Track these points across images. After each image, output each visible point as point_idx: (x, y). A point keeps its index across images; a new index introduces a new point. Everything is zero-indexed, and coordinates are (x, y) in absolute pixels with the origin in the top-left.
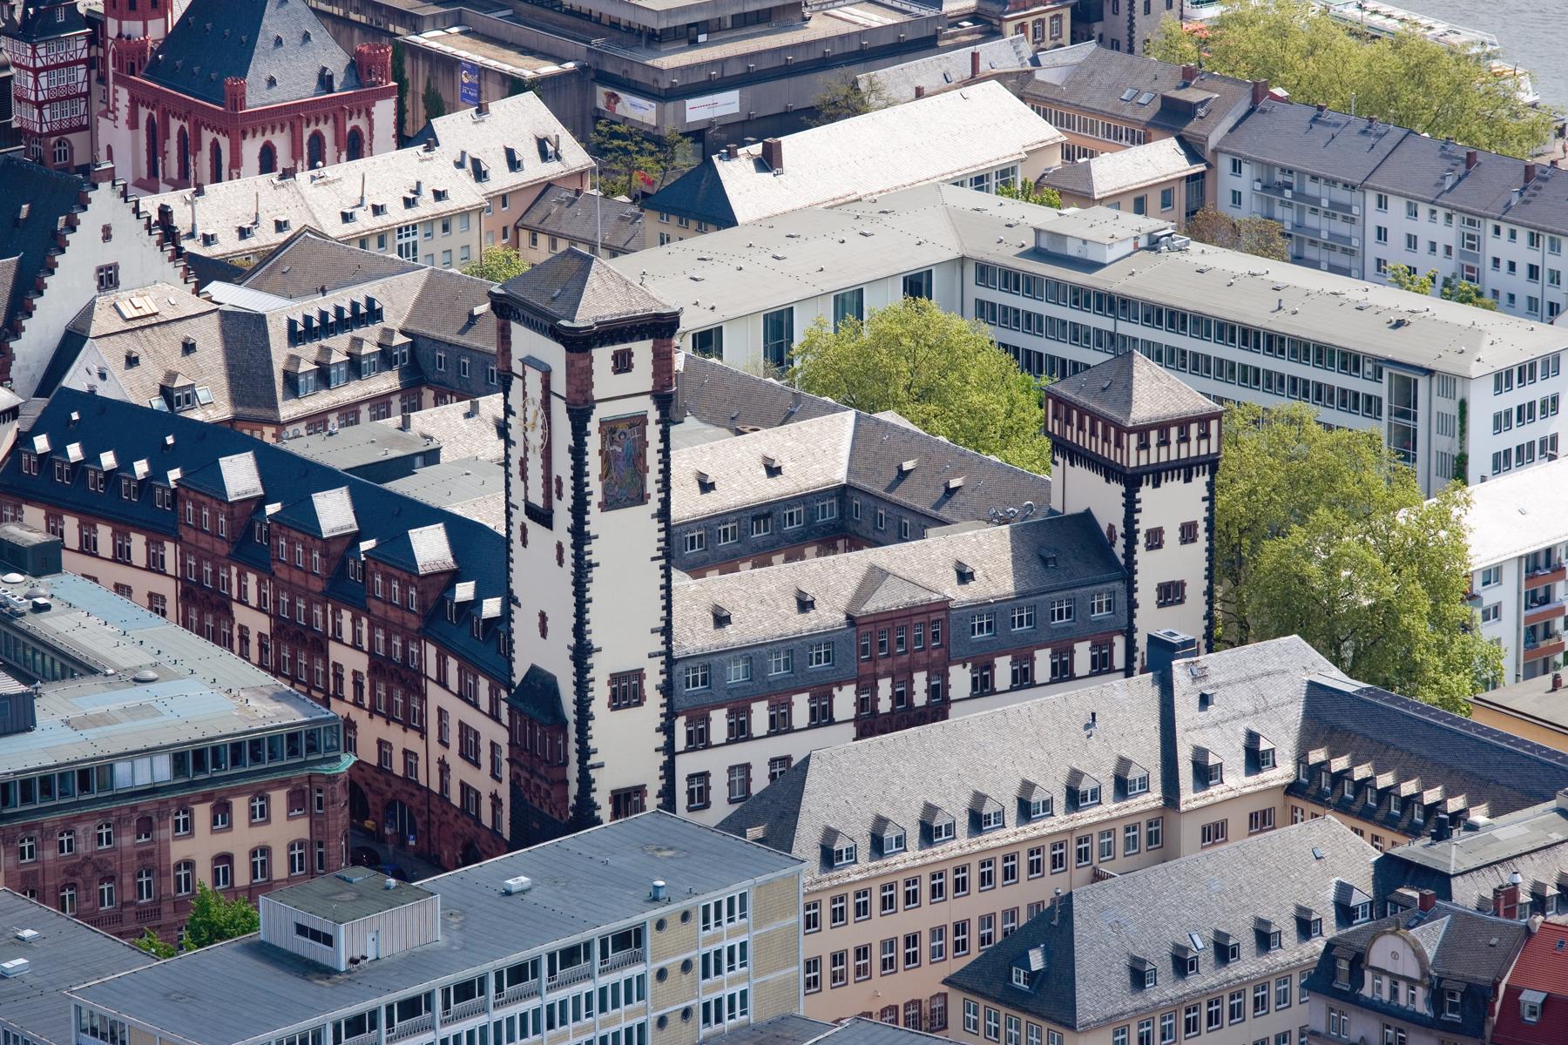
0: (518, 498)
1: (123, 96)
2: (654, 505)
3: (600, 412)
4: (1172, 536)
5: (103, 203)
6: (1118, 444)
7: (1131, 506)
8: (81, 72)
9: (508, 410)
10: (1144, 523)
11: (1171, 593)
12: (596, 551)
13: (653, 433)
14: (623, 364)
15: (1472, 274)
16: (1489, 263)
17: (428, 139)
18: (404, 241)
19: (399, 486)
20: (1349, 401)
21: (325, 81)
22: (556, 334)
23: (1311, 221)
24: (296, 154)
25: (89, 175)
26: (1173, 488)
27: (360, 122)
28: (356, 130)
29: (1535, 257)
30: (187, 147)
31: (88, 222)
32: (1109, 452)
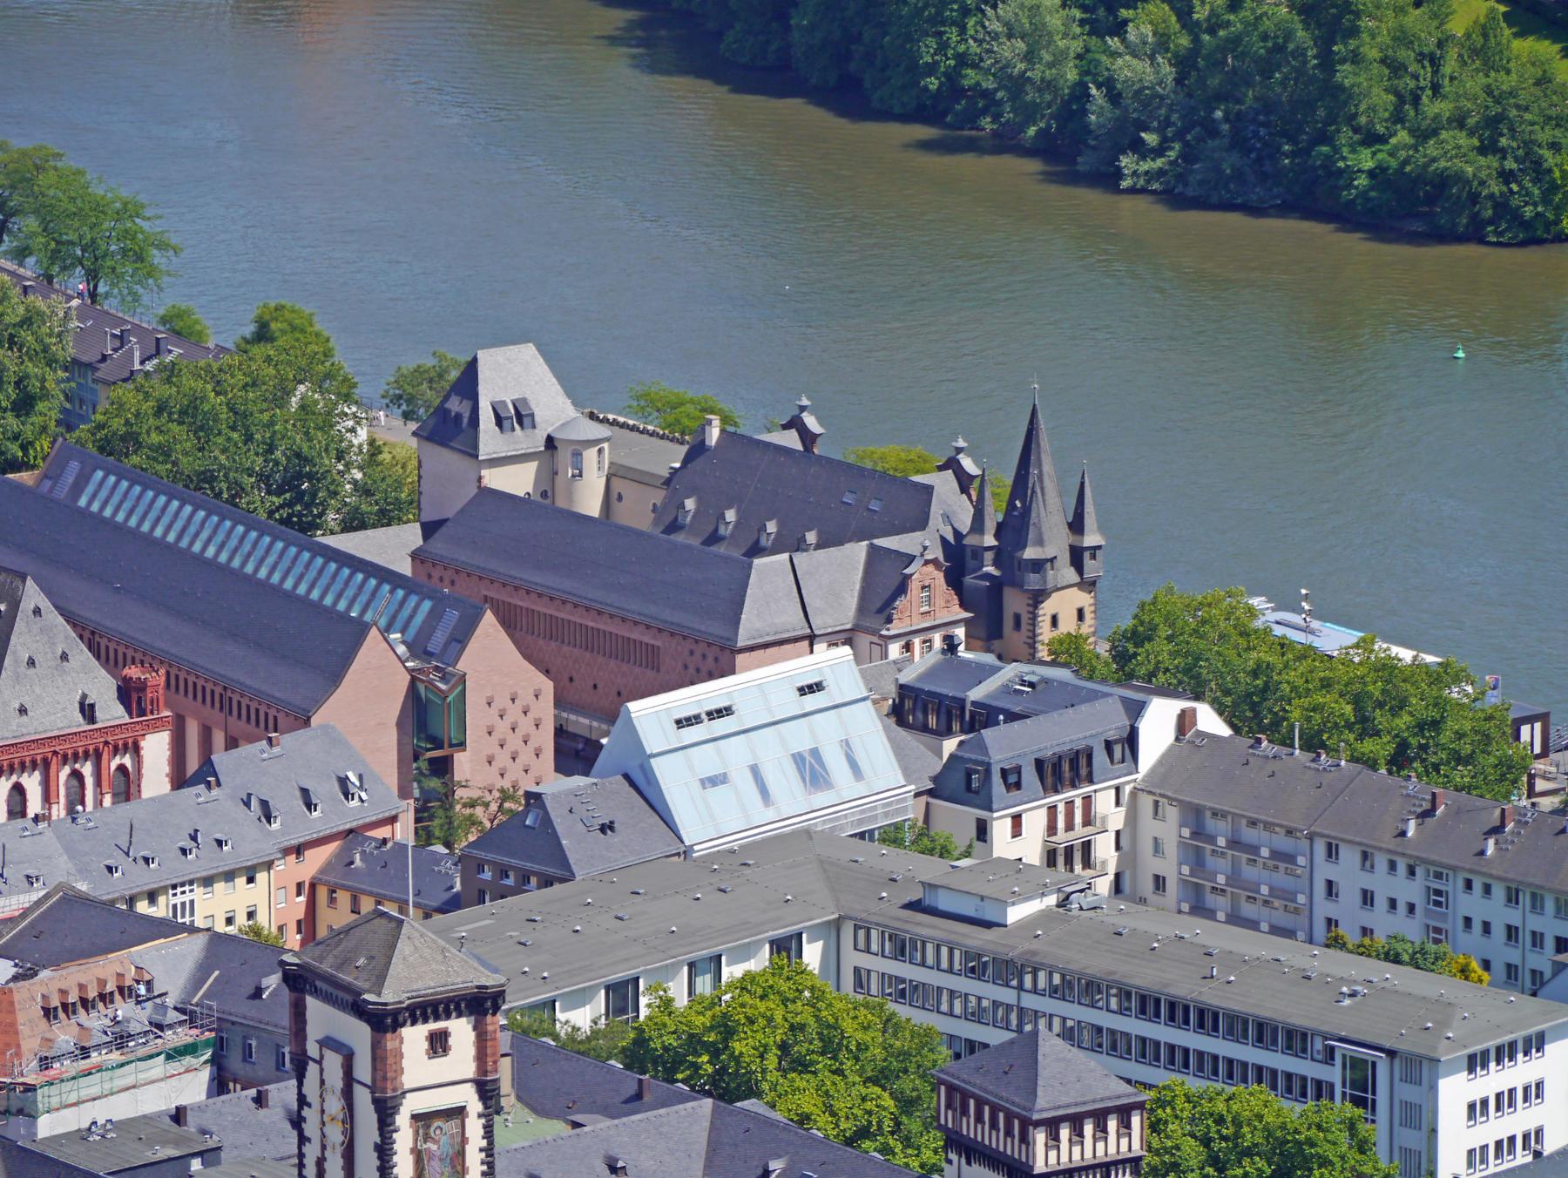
3: (412, 1104)
6: (1025, 1139)
9: (302, 1101)
14: (438, 1044)
16: (1460, 923)
17: (207, 774)
18: (178, 900)
20: (1294, 1086)
21: (88, 711)
22: (359, 1009)
23: (1249, 872)
24: (47, 799)
27: (127, 761)
28: (122, 769)
29: (1514, 917)
32: (1011, 1148)
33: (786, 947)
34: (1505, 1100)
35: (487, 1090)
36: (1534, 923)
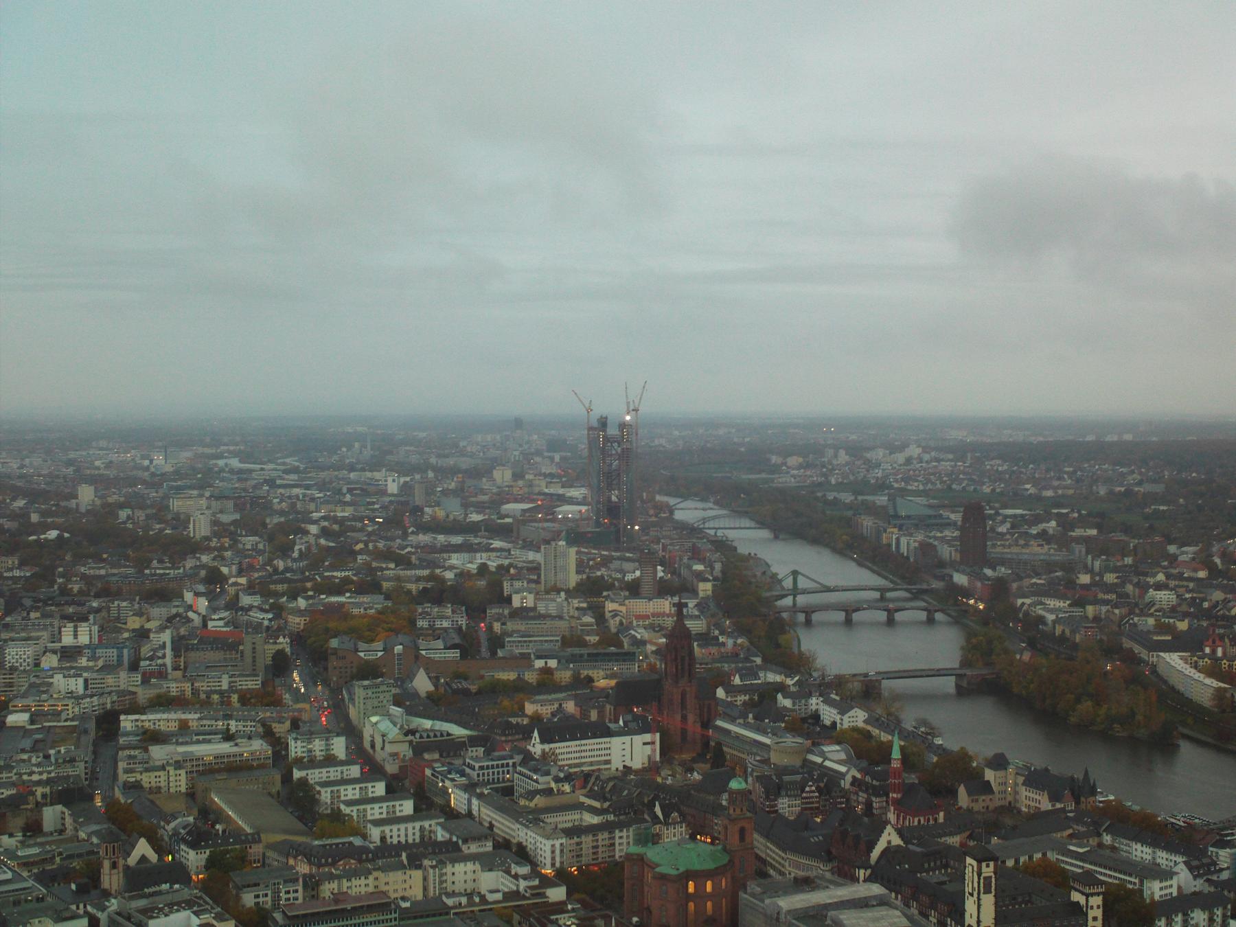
0: (966, 890)
1: (892, 808)
2: (993, 894)
3: (983, 875)
4: (1095, 907)
5: (889, 829)
7: (1087, 901)
8: (884, 803)
10: (1090, 904)
11: (1095, 919)
12: (982, 902)
13: (993, 880)
14: (988, 866)
15: (1154, 859)
19: (944, 887)
22: (975, 859)
25: (887, 822)
26: (1095, 898)
30: (904, 819)
31: (886, 832)
33: (1044, 854)
34: (1166, 887)
35: (995, 873)
36: (1171, 858)
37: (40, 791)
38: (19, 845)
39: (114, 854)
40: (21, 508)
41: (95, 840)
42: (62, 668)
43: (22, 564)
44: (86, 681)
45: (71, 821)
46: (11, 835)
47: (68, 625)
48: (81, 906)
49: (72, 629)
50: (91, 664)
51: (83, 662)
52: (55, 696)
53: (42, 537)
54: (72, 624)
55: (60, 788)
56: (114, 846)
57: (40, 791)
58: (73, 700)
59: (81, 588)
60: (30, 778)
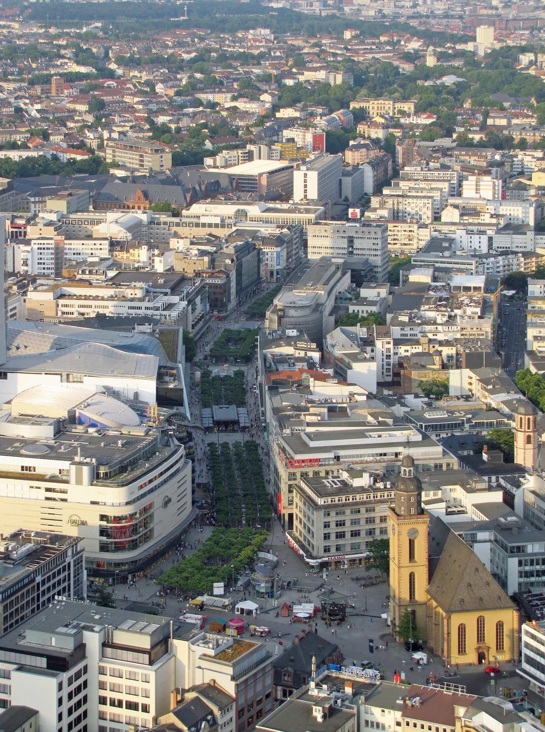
37: (447, 351)
38: (425, 406)
39: (529, 428)
40: (416, 51)
41: (506, 410)
42: (464, 225)
43: (419, 111)
44: (490, 239)
45: (480, 387)
46: (417, 396)
47: (470, 178)
48: (494, 478)
49: (474, 183)
50: (494, 221)
51: (486, 219)
52: (458, 253)
53: (438, 82)
54: (474, 178)
55: (467, 351)
56: (529, 419)
57: (447, 351)
58: (477, 259)
59: (481, 138)
60: (435, 337)
